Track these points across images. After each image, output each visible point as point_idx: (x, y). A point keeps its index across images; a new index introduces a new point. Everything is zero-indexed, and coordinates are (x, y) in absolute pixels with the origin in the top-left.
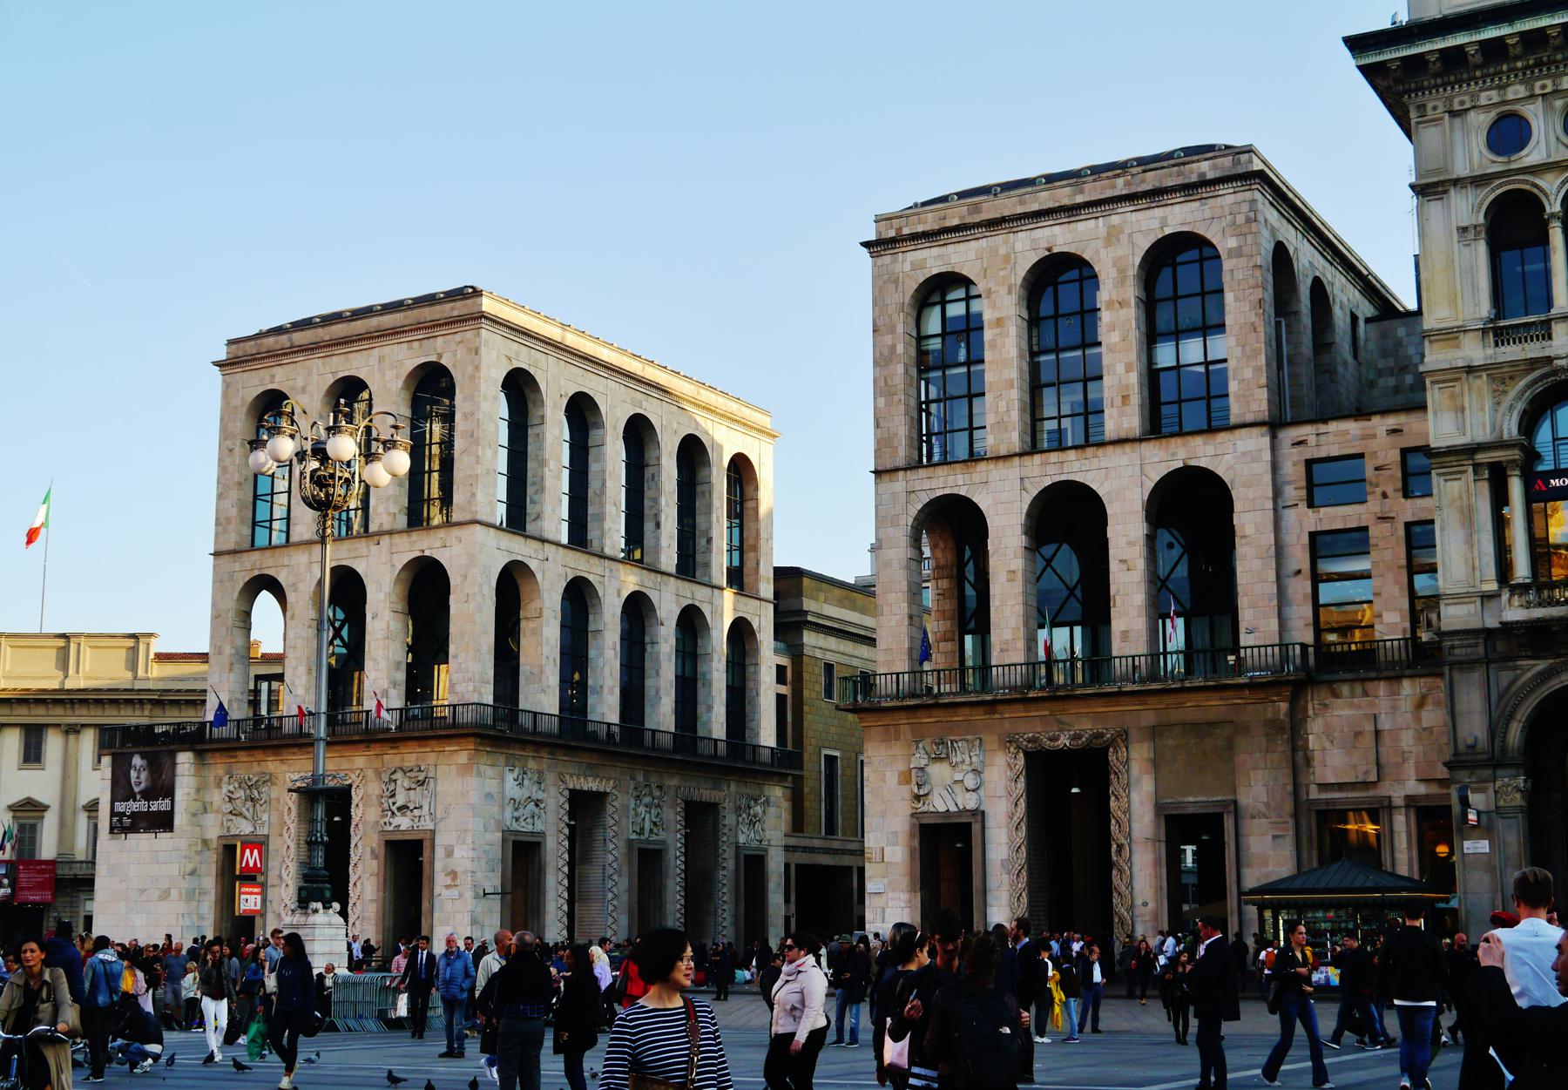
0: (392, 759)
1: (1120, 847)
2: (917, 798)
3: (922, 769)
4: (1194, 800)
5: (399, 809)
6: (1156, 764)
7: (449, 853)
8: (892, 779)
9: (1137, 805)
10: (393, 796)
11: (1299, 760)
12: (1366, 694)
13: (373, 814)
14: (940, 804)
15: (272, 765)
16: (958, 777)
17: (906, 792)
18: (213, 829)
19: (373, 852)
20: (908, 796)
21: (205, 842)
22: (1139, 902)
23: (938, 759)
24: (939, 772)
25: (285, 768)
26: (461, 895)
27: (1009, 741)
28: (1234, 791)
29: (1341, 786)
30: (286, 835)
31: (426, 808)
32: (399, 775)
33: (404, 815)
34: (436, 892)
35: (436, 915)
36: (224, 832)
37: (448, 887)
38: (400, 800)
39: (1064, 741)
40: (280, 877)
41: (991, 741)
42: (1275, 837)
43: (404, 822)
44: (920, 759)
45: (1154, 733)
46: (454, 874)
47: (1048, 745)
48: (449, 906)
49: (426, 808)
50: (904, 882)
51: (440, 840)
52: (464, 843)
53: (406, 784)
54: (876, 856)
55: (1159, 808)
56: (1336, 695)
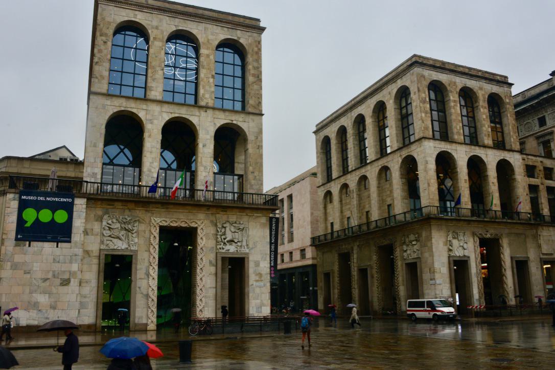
0: (222, 217)
1: (505, 270)
2: (450, 250)
3: (450, 241)
4: (520, 255)
5: (228, 241)
6: (510, 244)
7: (257, 264)
8: (441, 244)
9: (506, 255)
10: (224, 234)
11: (539, 246)
12: (548, 230)
13: (211, 243)
14: (458, 253)
15: (140, 213)
16: (461, 244)
17: (446, 248)
18: (94, 245)
19: (210, 262)
20: (447, 250)
21: (87, 253)
22: (509, 286)
23: (454, 238)
24: (455, 242)
25: (149, 214)
26: (264, 285)
27: (474, 234)
28: (527, 255)
29: (546, 254)
30: (152, 251)
31: (244, 243)
32: (227, 225)
33: (231, 244)
34: (251, 283)
35: (251, 295)
36: (103, 247)
37: (257, 281)
38: (229, 237)
39: (488, 236)
40: (148, 275)
41: (468, 233)
42: (537, 268)
43: (232, 248)
44: (450, 238)
45: (509, 235)
46: (260, 275)
47: (485, 236)
48: (258, 290)
49: (244, 243)
50: (448, 280)
51: (251, 258)
52: (265, 260)
53: (233, 230)
54: (438, 270)
55: (512, 258)
56: (543, 229)
